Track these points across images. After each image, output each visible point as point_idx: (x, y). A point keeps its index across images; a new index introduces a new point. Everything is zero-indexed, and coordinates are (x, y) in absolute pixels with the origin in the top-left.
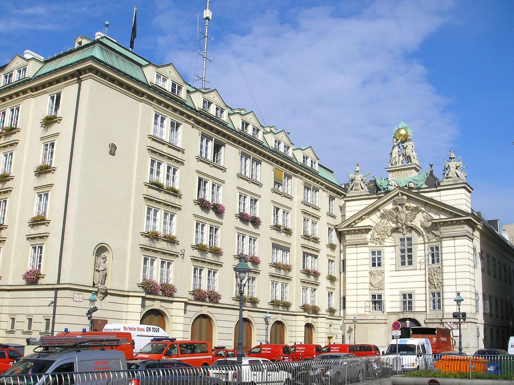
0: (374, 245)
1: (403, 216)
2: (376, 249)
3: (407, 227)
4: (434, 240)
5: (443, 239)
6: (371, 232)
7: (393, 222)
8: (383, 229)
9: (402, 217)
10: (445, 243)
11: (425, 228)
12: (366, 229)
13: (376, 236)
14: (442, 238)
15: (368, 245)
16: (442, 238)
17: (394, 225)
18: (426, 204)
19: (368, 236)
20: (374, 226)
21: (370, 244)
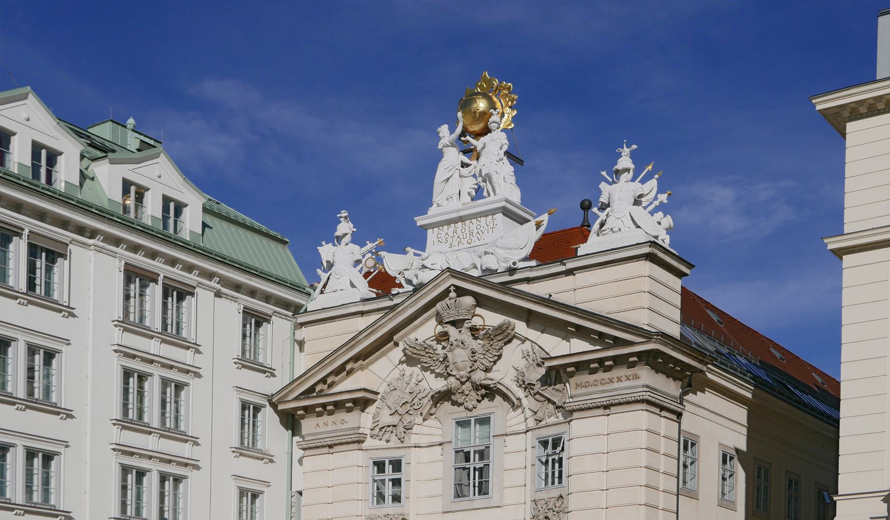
0: (383, 444)
1: (460, 356)
2: (386, 455)
3: (477, 387)
4: (553, 420)
5: (575, 415)
6: (371, 409)
7: (438, 375)
8: (409, 398)
9: (459, 360)
10: (580, 426)
11: (528, 387)
12: (355, 401)
13: (386, 419)
14: (572, 412)
15: (364, 445)
16: (572, 412)
17: (439, 385)
18: (529, 317)
19: (365, 420)
20: (381, 391)
21: (369, 443)
